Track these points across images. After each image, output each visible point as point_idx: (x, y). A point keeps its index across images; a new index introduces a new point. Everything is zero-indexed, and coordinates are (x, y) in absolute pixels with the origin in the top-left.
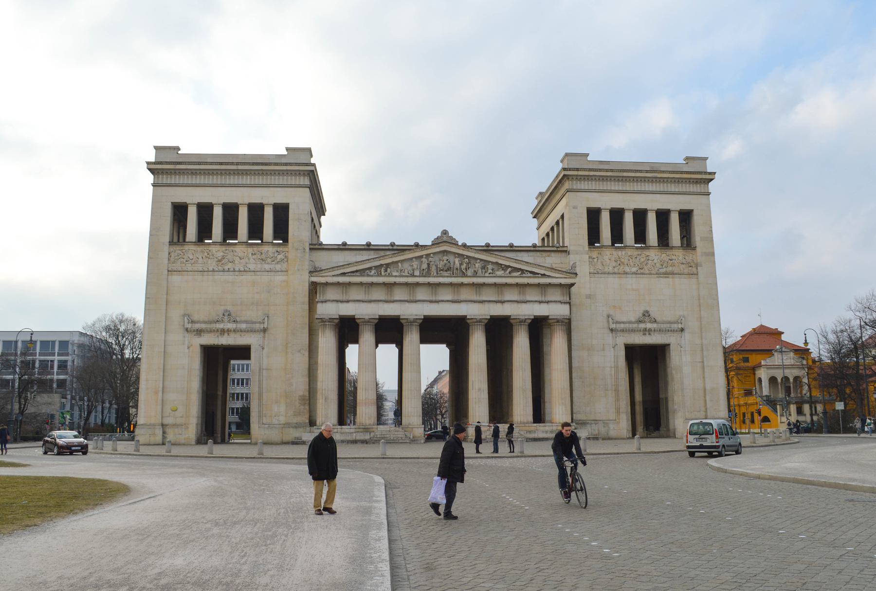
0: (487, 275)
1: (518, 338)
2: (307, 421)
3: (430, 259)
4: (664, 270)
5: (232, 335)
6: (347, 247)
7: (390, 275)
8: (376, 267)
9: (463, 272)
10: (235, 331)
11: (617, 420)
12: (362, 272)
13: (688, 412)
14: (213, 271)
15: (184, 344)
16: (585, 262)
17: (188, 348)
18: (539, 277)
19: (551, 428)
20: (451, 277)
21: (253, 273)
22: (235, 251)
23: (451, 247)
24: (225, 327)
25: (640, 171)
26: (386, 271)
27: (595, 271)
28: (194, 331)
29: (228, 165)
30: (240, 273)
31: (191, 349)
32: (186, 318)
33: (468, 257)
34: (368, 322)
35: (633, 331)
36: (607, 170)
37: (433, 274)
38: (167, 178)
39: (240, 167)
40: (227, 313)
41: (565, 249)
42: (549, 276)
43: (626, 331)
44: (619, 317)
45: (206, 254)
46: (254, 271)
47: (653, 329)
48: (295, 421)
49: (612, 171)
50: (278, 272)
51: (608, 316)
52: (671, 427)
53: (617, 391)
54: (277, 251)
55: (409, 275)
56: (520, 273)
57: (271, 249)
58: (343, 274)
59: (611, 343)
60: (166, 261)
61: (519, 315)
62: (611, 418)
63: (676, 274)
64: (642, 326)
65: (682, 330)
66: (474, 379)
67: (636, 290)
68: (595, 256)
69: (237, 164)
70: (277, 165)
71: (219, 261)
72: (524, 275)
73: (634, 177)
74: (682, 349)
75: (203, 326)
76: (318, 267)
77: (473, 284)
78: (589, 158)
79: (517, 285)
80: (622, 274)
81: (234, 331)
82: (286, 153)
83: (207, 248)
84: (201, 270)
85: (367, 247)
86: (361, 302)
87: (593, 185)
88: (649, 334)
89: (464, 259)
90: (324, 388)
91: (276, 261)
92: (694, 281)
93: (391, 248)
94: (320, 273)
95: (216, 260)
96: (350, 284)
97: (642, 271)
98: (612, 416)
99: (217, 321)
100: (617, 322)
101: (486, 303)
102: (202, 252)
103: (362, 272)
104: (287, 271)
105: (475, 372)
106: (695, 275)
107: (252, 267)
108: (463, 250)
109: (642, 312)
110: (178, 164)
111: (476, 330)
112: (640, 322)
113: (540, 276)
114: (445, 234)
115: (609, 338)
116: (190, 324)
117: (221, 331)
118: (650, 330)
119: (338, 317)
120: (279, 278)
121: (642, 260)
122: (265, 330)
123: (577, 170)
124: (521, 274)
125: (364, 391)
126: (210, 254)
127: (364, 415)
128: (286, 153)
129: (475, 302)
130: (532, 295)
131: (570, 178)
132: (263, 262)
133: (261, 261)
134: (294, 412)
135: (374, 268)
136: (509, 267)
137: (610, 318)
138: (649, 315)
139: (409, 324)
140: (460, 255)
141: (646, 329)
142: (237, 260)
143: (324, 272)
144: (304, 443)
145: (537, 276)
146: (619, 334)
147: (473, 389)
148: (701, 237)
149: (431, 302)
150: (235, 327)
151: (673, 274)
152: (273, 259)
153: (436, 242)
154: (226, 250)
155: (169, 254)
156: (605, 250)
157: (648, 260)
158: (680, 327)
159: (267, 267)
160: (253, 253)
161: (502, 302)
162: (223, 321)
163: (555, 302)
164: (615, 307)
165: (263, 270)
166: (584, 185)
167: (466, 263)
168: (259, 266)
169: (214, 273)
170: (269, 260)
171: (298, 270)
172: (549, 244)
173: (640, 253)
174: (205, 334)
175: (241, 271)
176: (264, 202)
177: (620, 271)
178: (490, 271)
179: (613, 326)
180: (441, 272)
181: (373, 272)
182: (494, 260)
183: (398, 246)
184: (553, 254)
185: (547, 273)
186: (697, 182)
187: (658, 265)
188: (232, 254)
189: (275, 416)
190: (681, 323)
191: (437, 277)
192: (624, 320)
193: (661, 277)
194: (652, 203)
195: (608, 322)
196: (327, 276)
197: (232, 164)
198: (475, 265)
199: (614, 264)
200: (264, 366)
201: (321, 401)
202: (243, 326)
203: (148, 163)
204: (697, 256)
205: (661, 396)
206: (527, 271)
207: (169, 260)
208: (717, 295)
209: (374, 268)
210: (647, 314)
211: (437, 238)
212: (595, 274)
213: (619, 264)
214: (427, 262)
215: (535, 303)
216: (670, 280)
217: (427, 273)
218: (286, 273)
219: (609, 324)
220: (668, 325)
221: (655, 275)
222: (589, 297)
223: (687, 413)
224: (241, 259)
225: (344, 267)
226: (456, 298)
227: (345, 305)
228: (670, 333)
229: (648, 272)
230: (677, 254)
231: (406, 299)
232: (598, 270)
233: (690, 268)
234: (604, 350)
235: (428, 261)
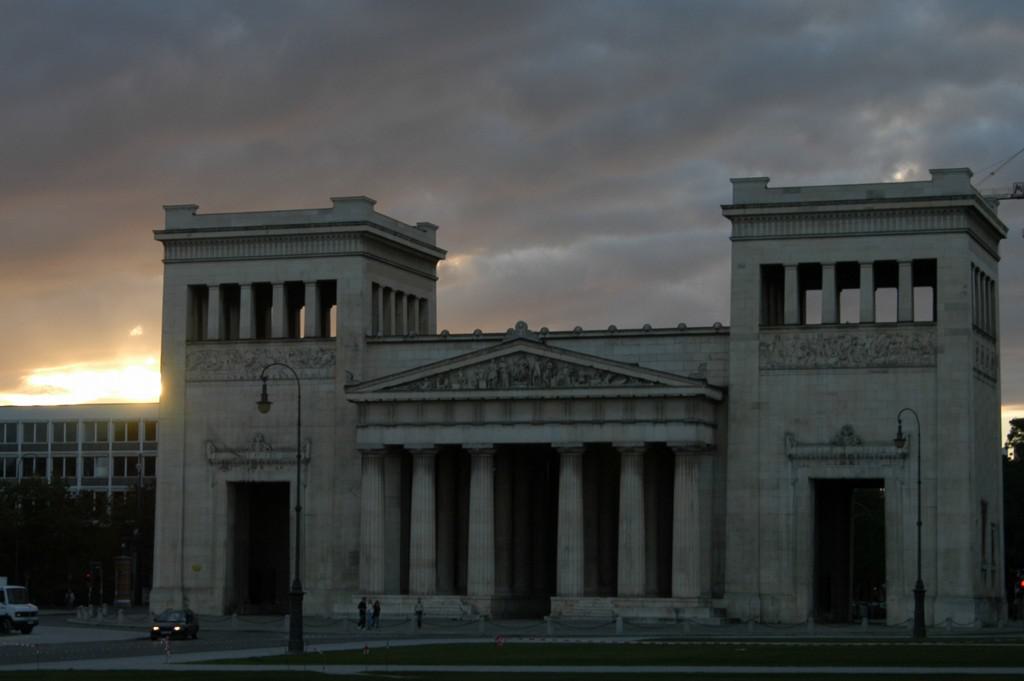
0: (577, 385)
4: (882, 359)
7: (449, 388)
8: (429, 377)
10: (269, 463)
14: (242, 379)
17: (213, 485)
18: (650, 387)
20: (527, 389)
27: (769, 366)
28: (219, 463)
33: (552, 360)
34: (422, 452)
35: (824, 458)
38: (181, 251)
39: (272, 232)
42: (665, 385)
45: (232, 356)
47: (856, 456)
51: (787, 434)
55: (470, 386)
56: (624, 381)
64: (838, 450)
68: (770, 342)
71: (249, 366)
78: (769, 185)
82: (330, 205)
87: (772, 229)
88: (851, 463)
95: (245, 364)
96: (396, 402)
97: (845, 363)
100: (798, 444)
104: (334, 378)
112: (834, 444)
116: (214, 454)
119: (381, 447)
121: (846, 345)
124: (627, 382)
128: (330, 205)
129: (562, 423)
130: (644, 412)
136: (607, 372)
138: (851, 434)
140: (540, 358)
149: (504, 424)
151: (894, 365)
156: (785, 331)
161: (601, 423)
162: (254, 450)
170: (311, 362)
176: (305, 279)
178: (582, 379)
179: (793, 451)
181: (426, 384)
185: (662, 380)
187: (872, 353)
191: (512, 389)
193: (873, 372)
195: (785, 445)
197: (260, 228)
199: (800, 353)
202: (279, 456)
203: (156, 232)
207: (187, 366)
210: (846, 432)
212: (769, 369)
213: (808, 354)
217: (496, 383)
222: (758, 406)
227: (392, 430)
229: (853, 364)
231: (470, 420)
233: (926, 356)
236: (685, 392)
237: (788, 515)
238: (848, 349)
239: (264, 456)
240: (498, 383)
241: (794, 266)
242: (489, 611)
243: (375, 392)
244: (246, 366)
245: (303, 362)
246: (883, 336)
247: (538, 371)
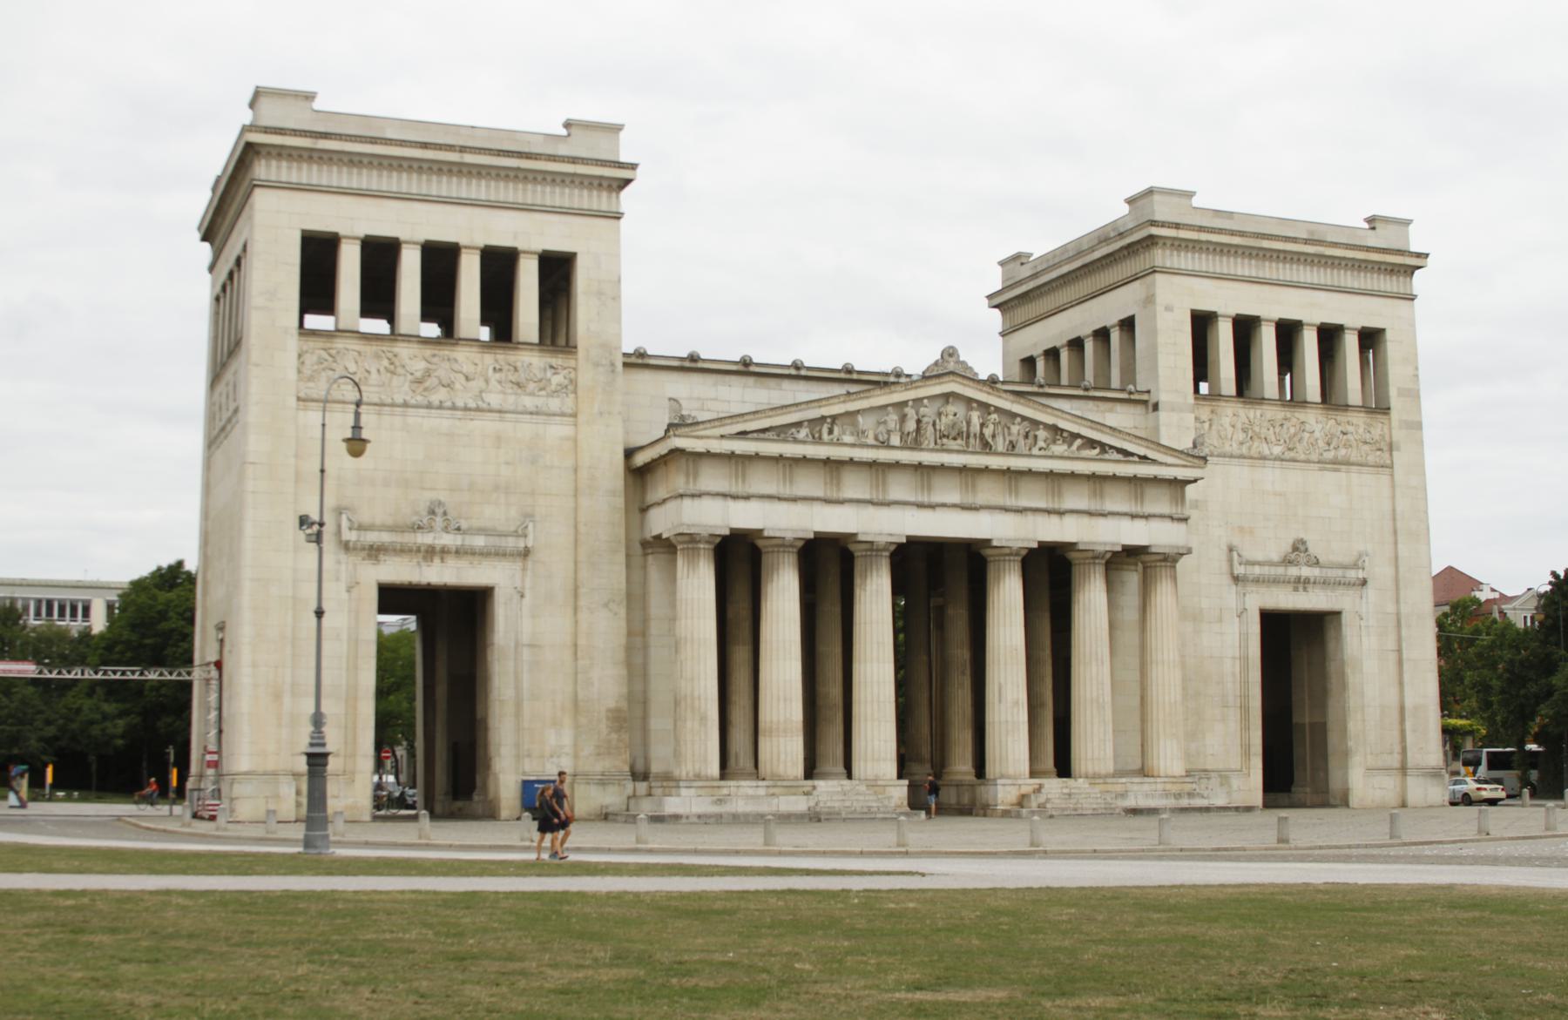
0: (1035, 451)
1: (1087, 594)
2: (627, 768)
3: (922, 410)
4: (1330, 455)
5: (451, 562)
6: (700, 365)
7: (839, 443)
8: (811, 421)
9: (987, 443)
10: (459, 552)
11: (1245, 771)
12: (781, 432)
13: (1372, 754)
14: (406, 405)
15: (338, 579)
16: (1188, 428)
17: (349, 590)
18: (1135, 462)
19: (1153, 787)
20: (964, 452)
21: (498, 415)
22: (456, 360)
23: (964, 385)
24: (437, 542)
25: (1294, 240)
26: (831, 432)
28: (363, 549)
29: (441, 149)
30: (468, 413)
31: (355, 591)
32: (344, 517)
33: (998, 410)
35: (1275, 581)
36: (1232, 233)
37: (928, 445)
40: (441, 511)
41: (1145, 397)
42: (1154, 461)
43: (1264, 581)
44: (1249, 554)
45: (385, 363)
46: (500, 411)
47: (1312, 580)
48: (599, 767)
49: (1243, 236)
50: (554, 415)
51: (1231, 550)
52: (1335, 783)
53: (1245, 709)
54: (552, 367)
55: (874, 442)
56: (1097, 451)
57: (533, 361)
58: (743, 434)
59: (1235, 607)
60: (292, 375)
61: (1094, 543)
62: (1233, 767)
63: (1353, 464)
64: (1293, 571)
65: (1364, 583)
66: (1002, 681)
67: (1280, 495)
69: (463, 149)
70: (555, 161)
71: (419, 382)
72: (1106, 456)
73: (1279, 251)
74: (1363, 623)
75: (386, 538)
76: (689, 416)
77: (1008, 473)
79: (1093, 478)
80: (1255, 459)
81: (457, 552)
82: (564, 132)
83: (389, 349)
84: (376, 400)
85: (740, 368)
86: (776, 501)
88: (1305, 589)
89: (989, 414)
90: (696, 694)
91: (548, 389)
92: (1384, 479)
93: (793, 372)
94: (693, 428)
95: (410, 377)
96: (757, 457)
98: (1235, 762)
99: (420, 528)
101: (1029, 513)
102: (377, 356)
103: (781, 432)
105: (1006, 664)
106: (1387, 467)
107: (494, 400)
108: (989, 393)
109: (1291, 542)
110: (322, 138)
111: (1007, 571)
113: (1136, 459)
114: (951, 355)
115: (1230, 595)
117: (427, 552)
118: (1307, 581)
120: (558, 430)
121: (1292, 430)
122: (526, 553)
123: (1177, 226)
125: (782, 703)
126: (397, 364)
127: (782, 757)
129: (1006, 509)
130: (1117, 501)
131: (1161, 242)
132: (519, 391)
133: (515, 387)
134: (598, 747)
135: (806, 423)
136: (1078, 436)
137: (1235, 554)
138: (1306, 550)
139: (874, 553)
140: (984, 407)
141: (1299, 578)
142: (459, 381)
143: (701, 426)
144: (587, 819)
145: (1131, 458)
146: (1251, 588)
147: (1000, 701)
148: (1399, 389)
149: (920, 506)
150: (459, 542)
151: (1348, 463)
152: (543, 384)
153: (935, 373)
154: (434, 356)
155: (300, 356)
156: (1224, 404)
157: (1304, 431)
158: (1361, 576)
159: (529, 402)
160: (498, 367)
161: (1060, 513)
162: (431, 529)
163: (1162, 516)
164: (1241, 529)
165: (520, 408)
166: (1184, 261)
167: (994, 424)
168: (511, 399)
169: (405, 409)
170: (531, 386)
171: (601, 414)
172: (1109, 379)
173: (1289, 415)
174: (387, 558)
175: (470, 410)
176: (520, 245)
177: (1254, 452)
179: (1240, 570)
180: (945, 440)
181: (803, 433)
182: (1050, 420)
183: (809, 369)
184: (1119, 407)
185: (1151, 454)
186: (1392, 271)
187: (1321, 444)
188: (446, 365)
189: (552, 756)
190: (1363, 569)
191: (937, 451)
192: (1260, 557)
194: (1312, 309)
196: (708, 437)
197: (450, 148)
198: (1009, 428)
199: (1241, 436)
200: (525, 639)
201: (689, 724)
202: (479, 541)
204: (1390, 429)
205: (1296, 719)
206: (1111, 447)
207: (299, 372)
208: (1426, 513)
209: (806, 423)
210: (1302, 548)
211: (936, 364)
214: (916, 417)
215: (1123, 517)
216: (1342, 476)
217: (915, 443)
218: (571, 419)
219: (1231, 566)
220: (1340, 572)
221: (1317, 465)
223: (1369, 757)
224: (467, 379)
225: (746, 418)
226: (969, 500)
227: (741, 504)
228: (1341, 587)
229: (1302, 457)
230: (1355, 421)
231: (867, 496)
232: (1212, 448)
233: (1378, 453)
234: (1220, 620)
235: (917, 413)
236: (1182, 473)
237: (1234, 658)
238: (1295, 435)
239: (449, 540)
240: (916, 439)
241: (1229, 317)
242: (906, 803)
243: (722, 436)
244: (412, 382)
245: (518, 384)
246: (1332, 422)
247: (976, 427)
